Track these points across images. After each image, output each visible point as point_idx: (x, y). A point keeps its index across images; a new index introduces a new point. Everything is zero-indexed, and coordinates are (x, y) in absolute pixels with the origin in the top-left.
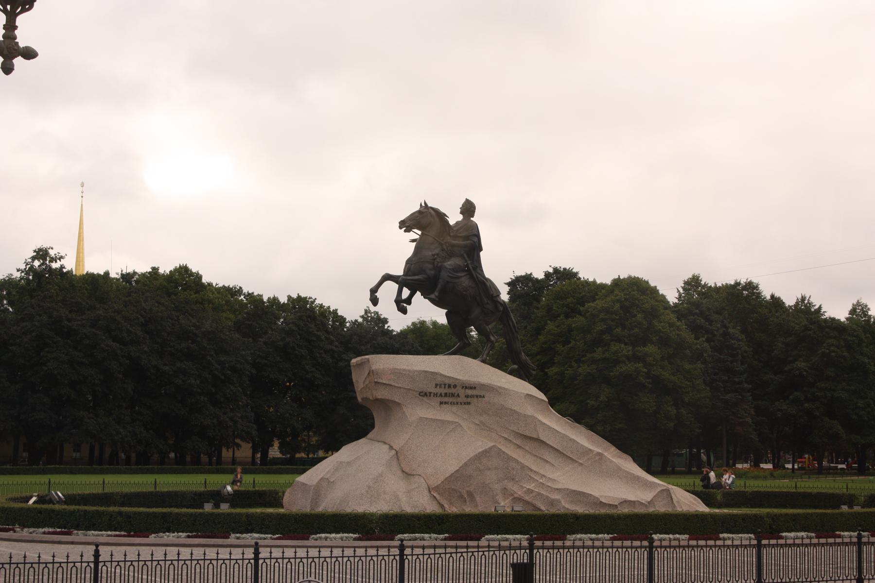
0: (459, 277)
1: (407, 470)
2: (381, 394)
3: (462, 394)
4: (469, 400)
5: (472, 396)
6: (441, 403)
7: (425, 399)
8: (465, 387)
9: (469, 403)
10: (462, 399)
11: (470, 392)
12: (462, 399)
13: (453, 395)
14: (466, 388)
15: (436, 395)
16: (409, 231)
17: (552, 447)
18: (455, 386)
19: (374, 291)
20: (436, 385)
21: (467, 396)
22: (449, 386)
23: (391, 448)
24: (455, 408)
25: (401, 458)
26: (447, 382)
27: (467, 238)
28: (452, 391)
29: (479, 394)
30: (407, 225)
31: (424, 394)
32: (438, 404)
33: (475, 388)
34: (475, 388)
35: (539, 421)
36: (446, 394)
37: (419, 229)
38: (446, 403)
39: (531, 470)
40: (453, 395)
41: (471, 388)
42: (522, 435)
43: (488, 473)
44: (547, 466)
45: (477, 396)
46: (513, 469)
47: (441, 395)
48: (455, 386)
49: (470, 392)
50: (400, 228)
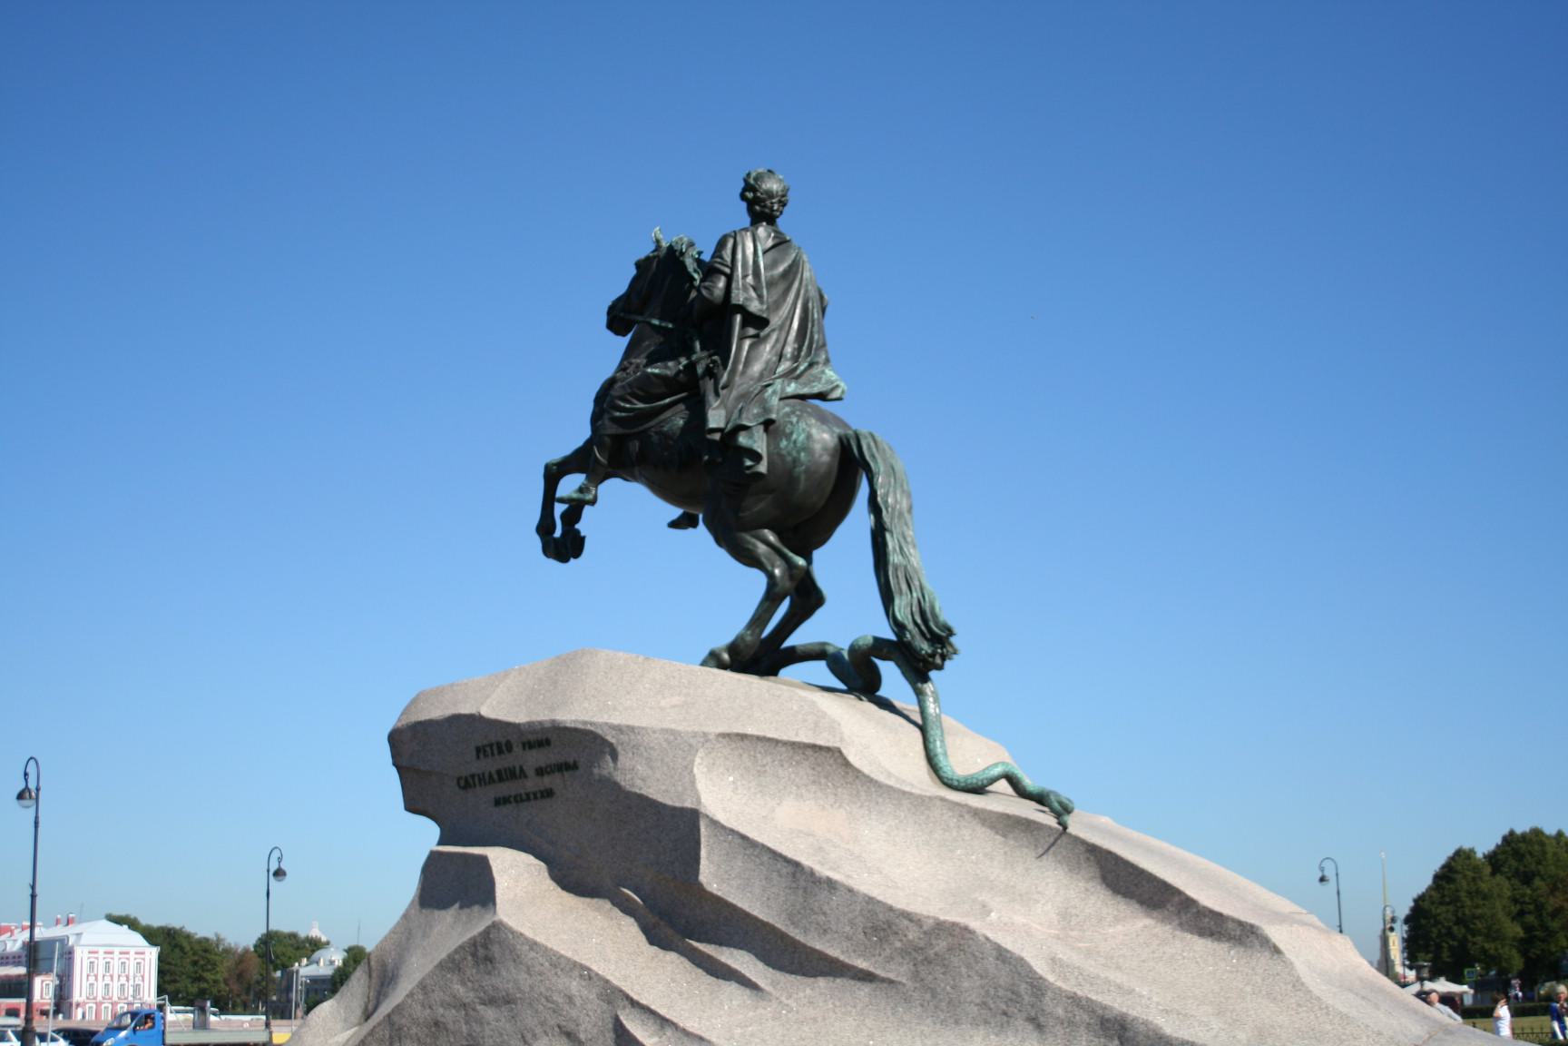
3: (531, 773)
4: (547, 781)
6: (498, 802)
8: (529, 745)
9: (548, 793)
10: (532, 784)
14: (529, 745)
15: (485, 780)
20: (478, 750)
21: (540, 772)
22: (499, 745)
29: (561, 759)
31: (466, 783)
35: (714, 823)
36: (499, 772)
39: (634, 1004)
43: (489, 1013)
44: (731, 988)
46: (570, 999)
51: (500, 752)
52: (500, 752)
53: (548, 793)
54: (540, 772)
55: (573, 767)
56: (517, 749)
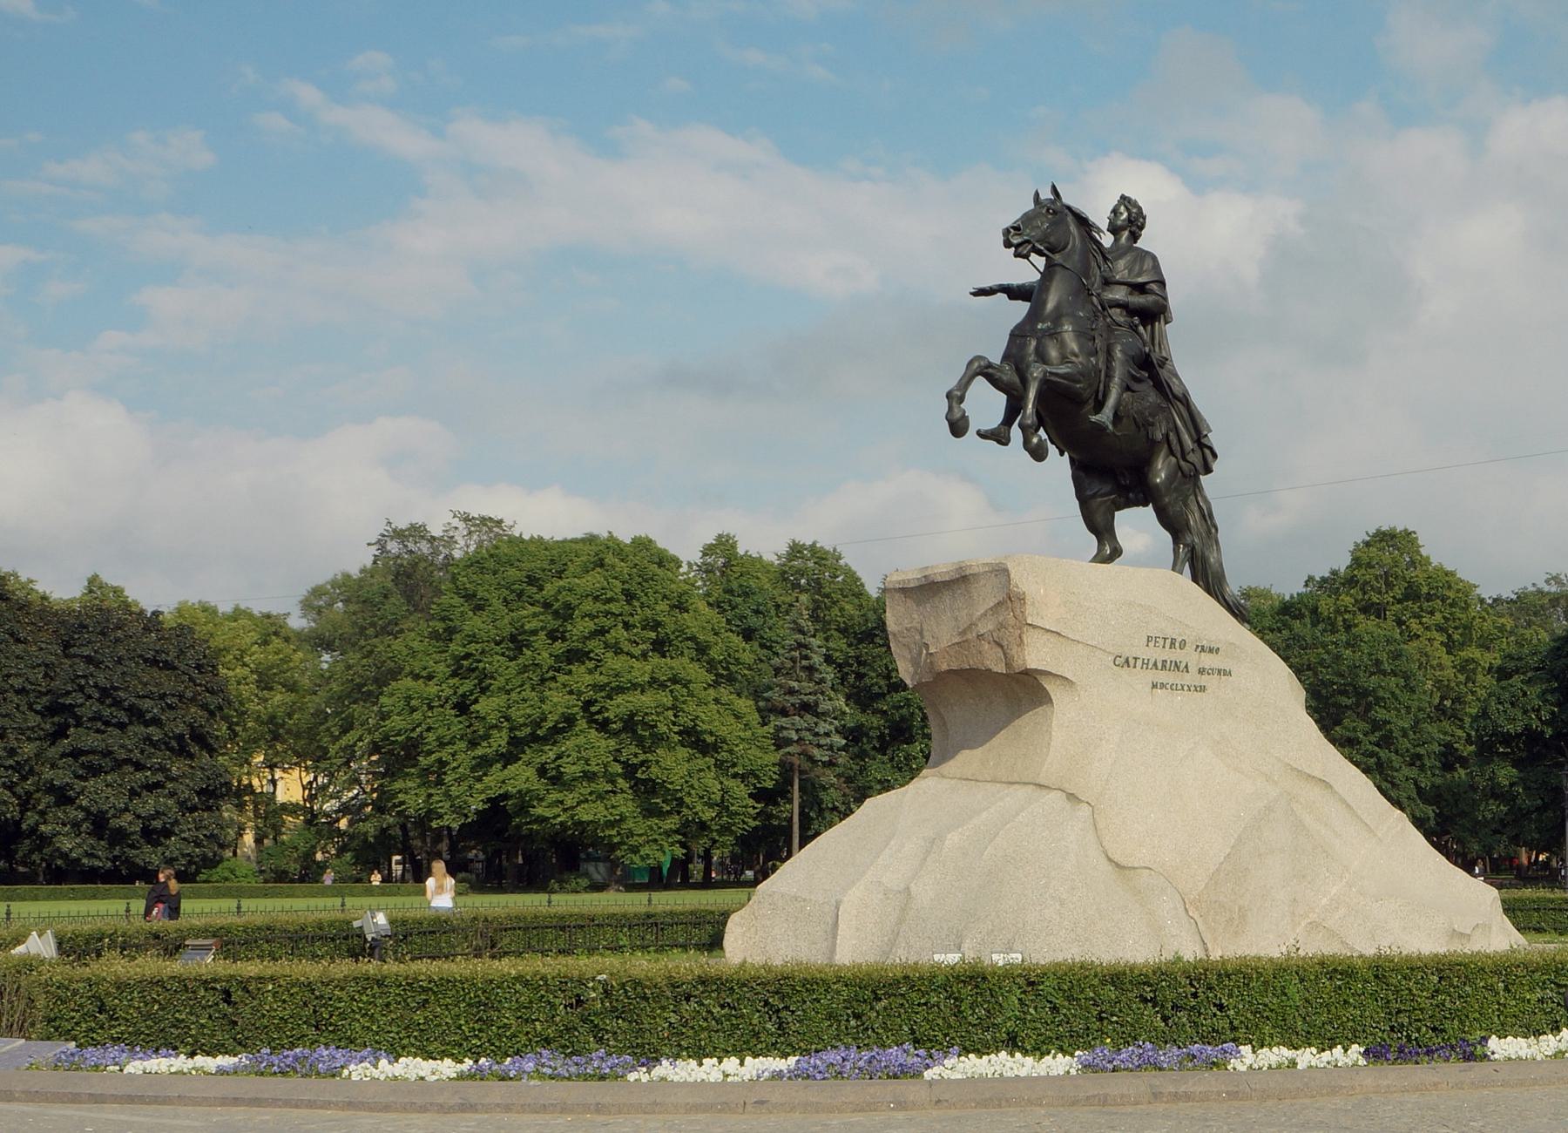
0: (1139, 380)
1: (1116, 858)
2: (1036, 655)
3: (1193, 669)
4: (1204, 680)
5: (1211, 672)
6: (1154, 686)
7: (1125, 671)
9: (1203, 689)
10: (1191, 678)
11: (1208, 661)
12: (1191, 678)
16: (1026, 257)
17: (1344, 801)
18: (1183, 644)
19: (955, 397)
20: (1149, 639)
21: (1201, 671)
23: (1072, 797)
24: (1179, 697)
25: (1101, 825)
27: (1141, 288)
30: (1019, 240)
37: (1040, 253)
38: (1163, 686)
41: (1211, 651)
42: (1293, 769)
47: (1155, 664)
48: (1183, 644)
49: (1208, 661)
50: (1008, 244)
54: (1201, 671)
55: (1228, 673)
56: (1189, 648)
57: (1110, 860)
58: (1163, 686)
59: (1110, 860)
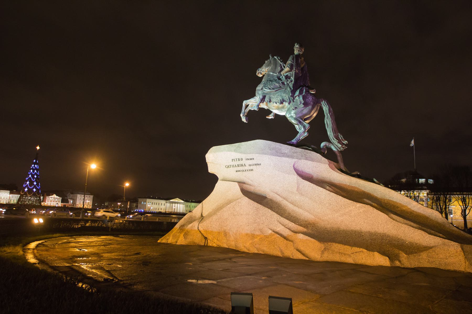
3: (247, 165)
4: (251, 168)
6: (237, 171)
9: (252, 170)
10: (247, 168)
13: (242, 165)
14: (248, 159)
15: (233, 166)
18: (242, 159)
20: (232, 160)
21: (250, 165)
26: (237, 158)
28: (241, 162)
32: (235, 172)
33: (253, 159)
34: (253, 159)
38: (239, 171)
40: (242, 165)
41: (251, 159)
45: (256, 165)
48: (242, 159)
51: (239, 160)
52: (239, 160)
53: (252, 170)
54: (250, 165)
56: (244, 160)
57: (202, 214)
58: (239, 171)
59: (202, 214)
